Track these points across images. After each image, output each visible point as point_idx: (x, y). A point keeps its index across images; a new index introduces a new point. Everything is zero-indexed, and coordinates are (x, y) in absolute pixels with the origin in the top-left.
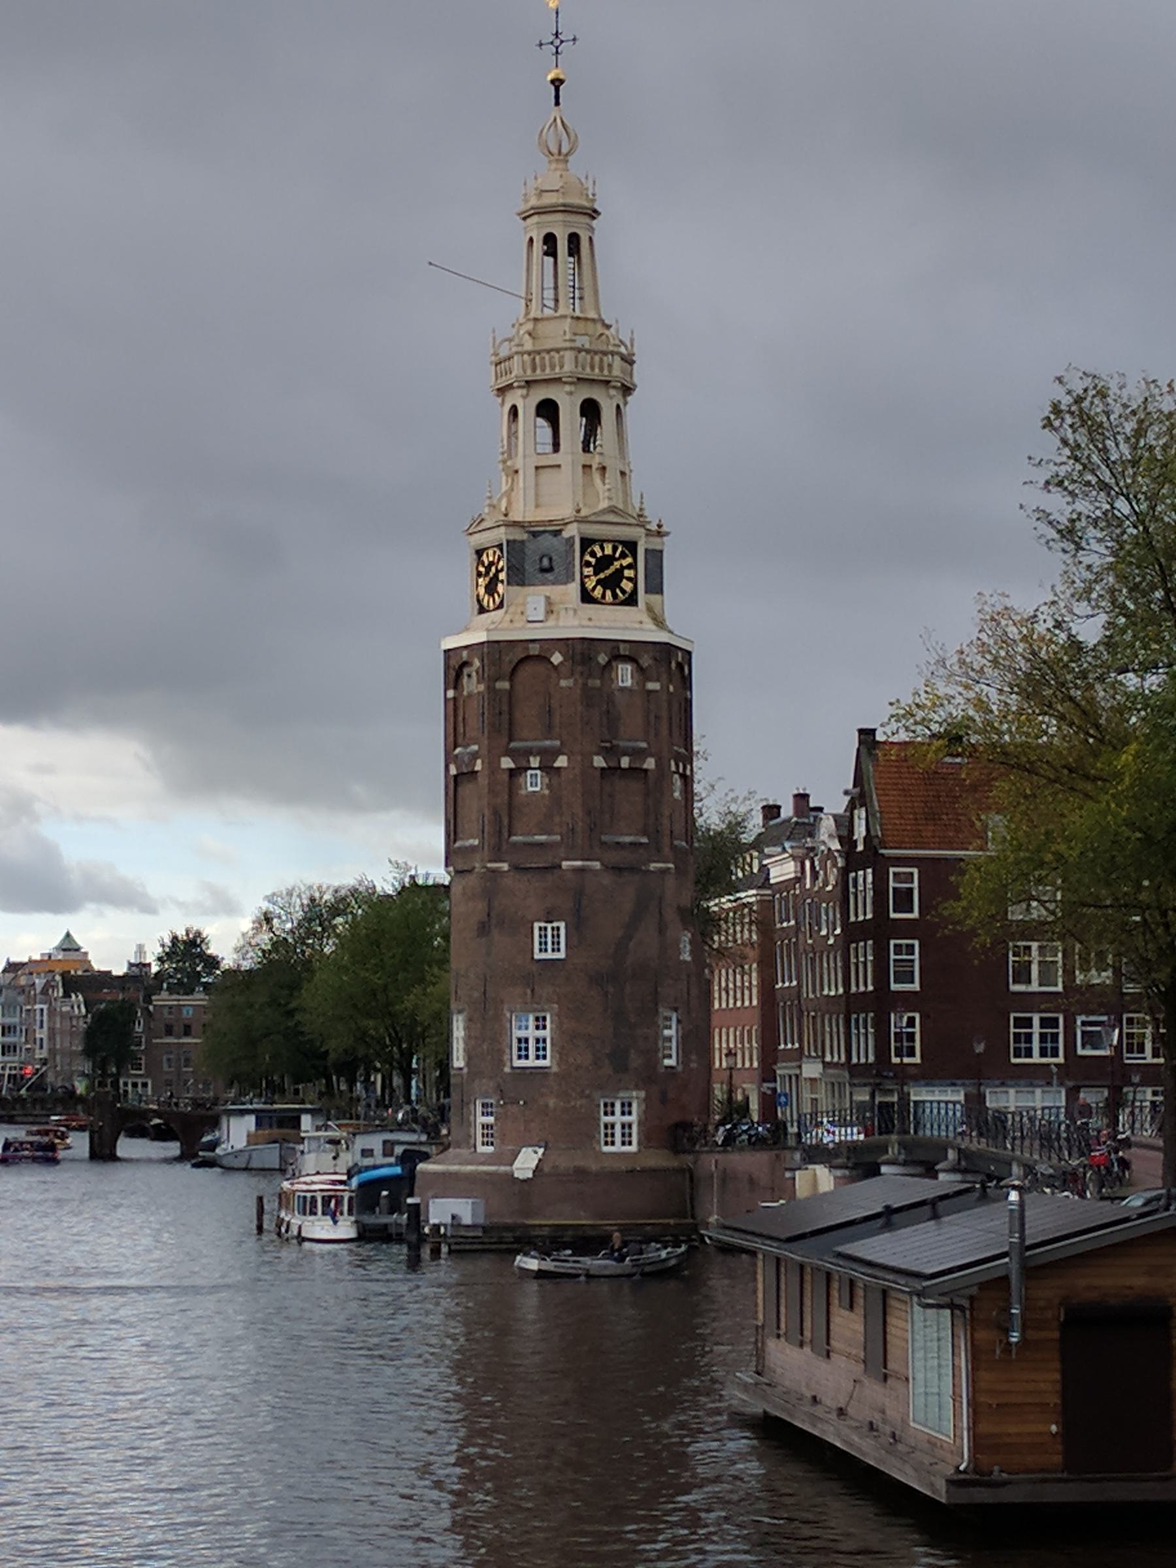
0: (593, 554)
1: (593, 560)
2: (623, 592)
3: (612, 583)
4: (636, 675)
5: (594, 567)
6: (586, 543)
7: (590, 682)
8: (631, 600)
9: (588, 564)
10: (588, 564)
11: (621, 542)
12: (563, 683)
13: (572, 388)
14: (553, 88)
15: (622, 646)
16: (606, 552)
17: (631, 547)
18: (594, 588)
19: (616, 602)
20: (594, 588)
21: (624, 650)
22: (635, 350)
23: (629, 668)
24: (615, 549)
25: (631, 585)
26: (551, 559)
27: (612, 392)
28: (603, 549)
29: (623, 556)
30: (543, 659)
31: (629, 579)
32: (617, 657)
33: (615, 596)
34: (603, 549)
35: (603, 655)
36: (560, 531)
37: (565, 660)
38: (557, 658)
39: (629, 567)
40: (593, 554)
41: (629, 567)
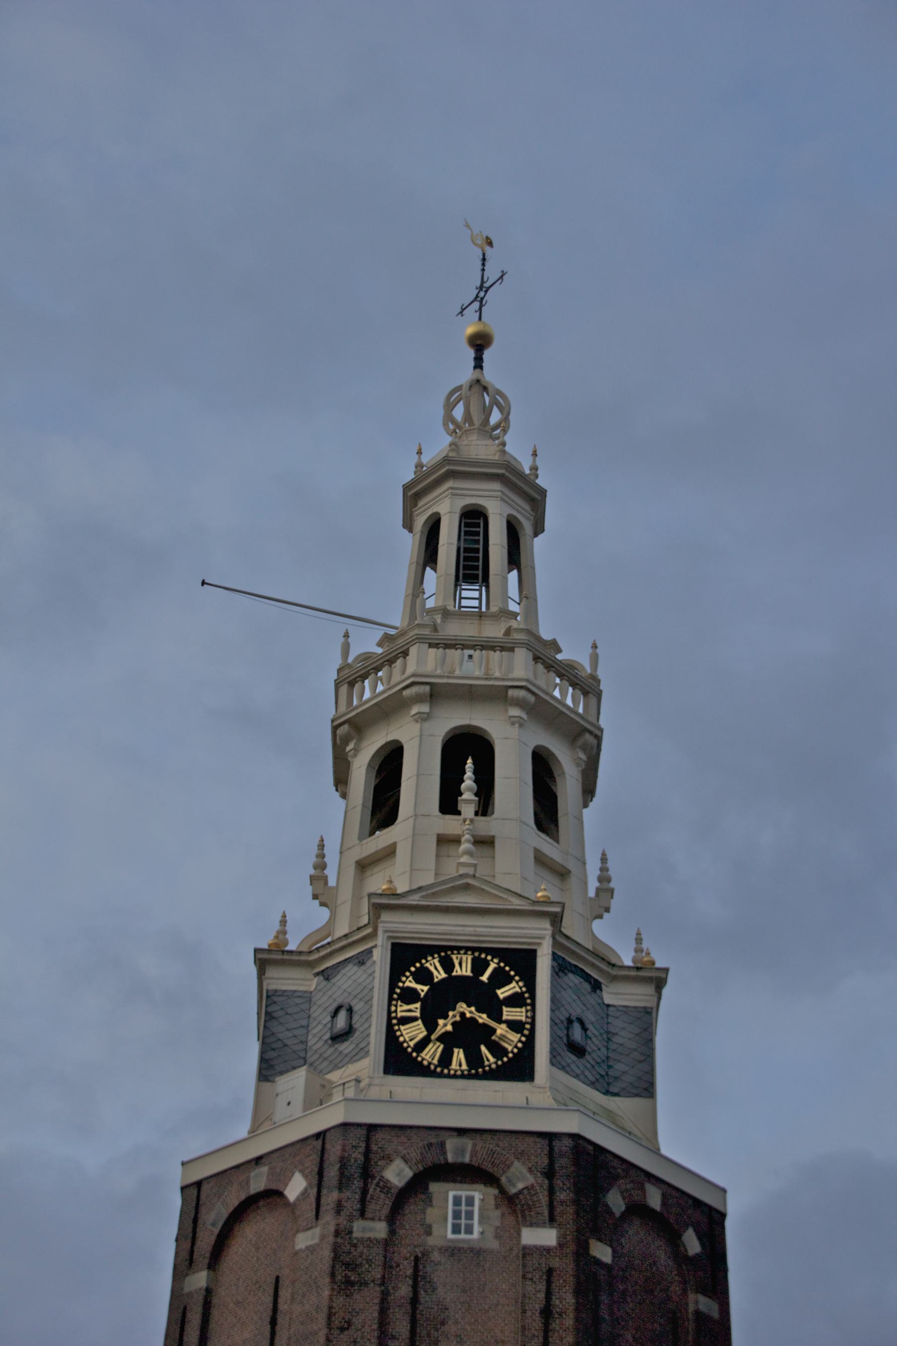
0: (424, 976)
1: (423, 989)
2: (497, 1050)
3: (469, 1036)
4: (495, 1215)
5: (425, 1002)
6: (405, 956)
7: (363, 1229)
8: (519, 1068)
9: (409, 996)
10: (409, 996)
11: (495, 952)
12: (303, 1241)
13: (425, 708)
14: (471, 353)
15: (451, 1144)
16: (457, 971)
17: (522, 961)
18: (421, 1045)
19: (476, 1070)
20: (421, 1045)
21: (455, 1151)
22: (600, 673)
23: (477, 1196)
24: (479, 966)
25: (514, 1037)
26: (350, 1010)
27: (515, 712)
28: (448, 965)
29: (500, 978)
30: (272, 1196)
31: (516, 1026)
32: (436, 1171)
33: (474, 1059)
34: (448, 965)
35: (398, 1164)
36: (369, 952)
37: (310, 1185)
38: (295, 1187)
39: (515, 1001)
40: (424, 976)
41: (515, 1001)
